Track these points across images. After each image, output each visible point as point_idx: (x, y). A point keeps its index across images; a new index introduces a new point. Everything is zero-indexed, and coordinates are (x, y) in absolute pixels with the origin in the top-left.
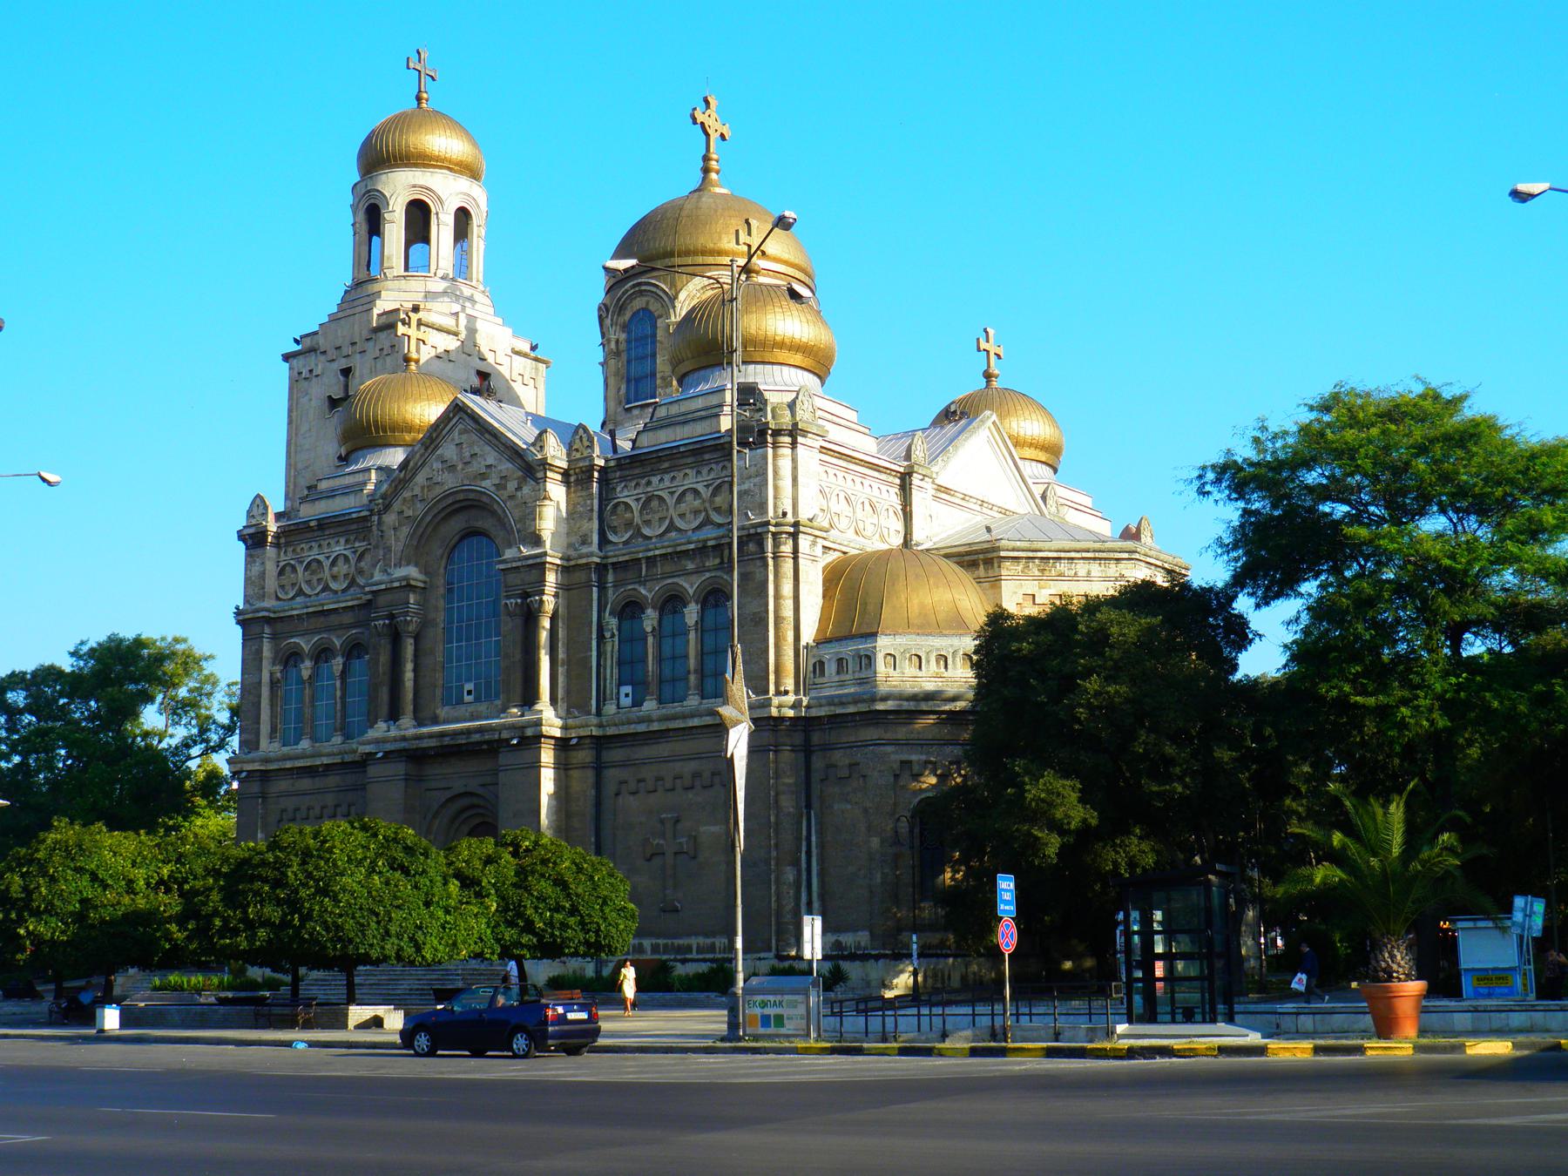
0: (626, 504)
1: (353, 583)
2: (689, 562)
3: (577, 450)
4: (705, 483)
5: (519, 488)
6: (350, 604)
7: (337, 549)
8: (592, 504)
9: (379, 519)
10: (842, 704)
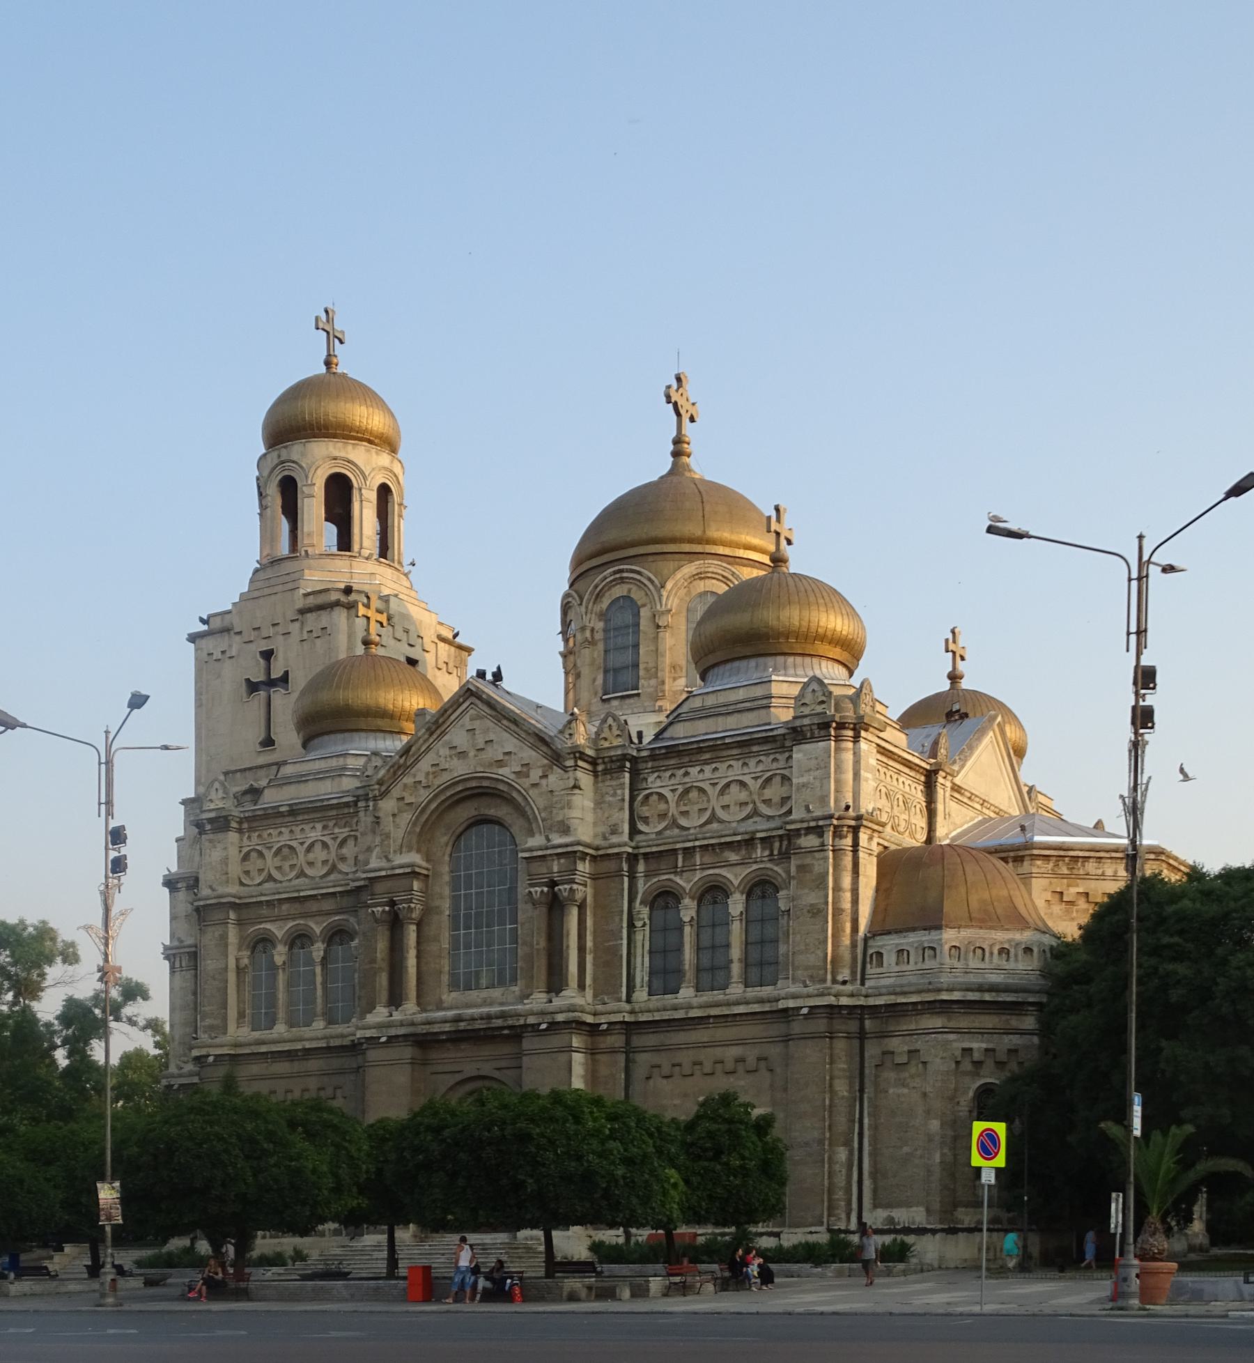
0: (659, 794)
1: (333, 869)
2: (733, 854)
3: (606, 739)
4: (753, 775)
5: (545, 776)
7: (312, 835)
8: (623, 794)
9: (375, 806)
10: (904, 993)
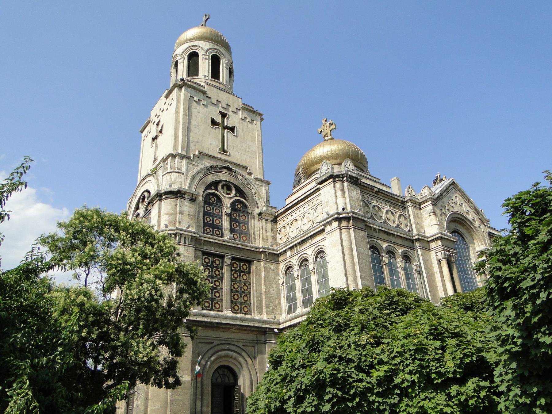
6: (403, 236)
